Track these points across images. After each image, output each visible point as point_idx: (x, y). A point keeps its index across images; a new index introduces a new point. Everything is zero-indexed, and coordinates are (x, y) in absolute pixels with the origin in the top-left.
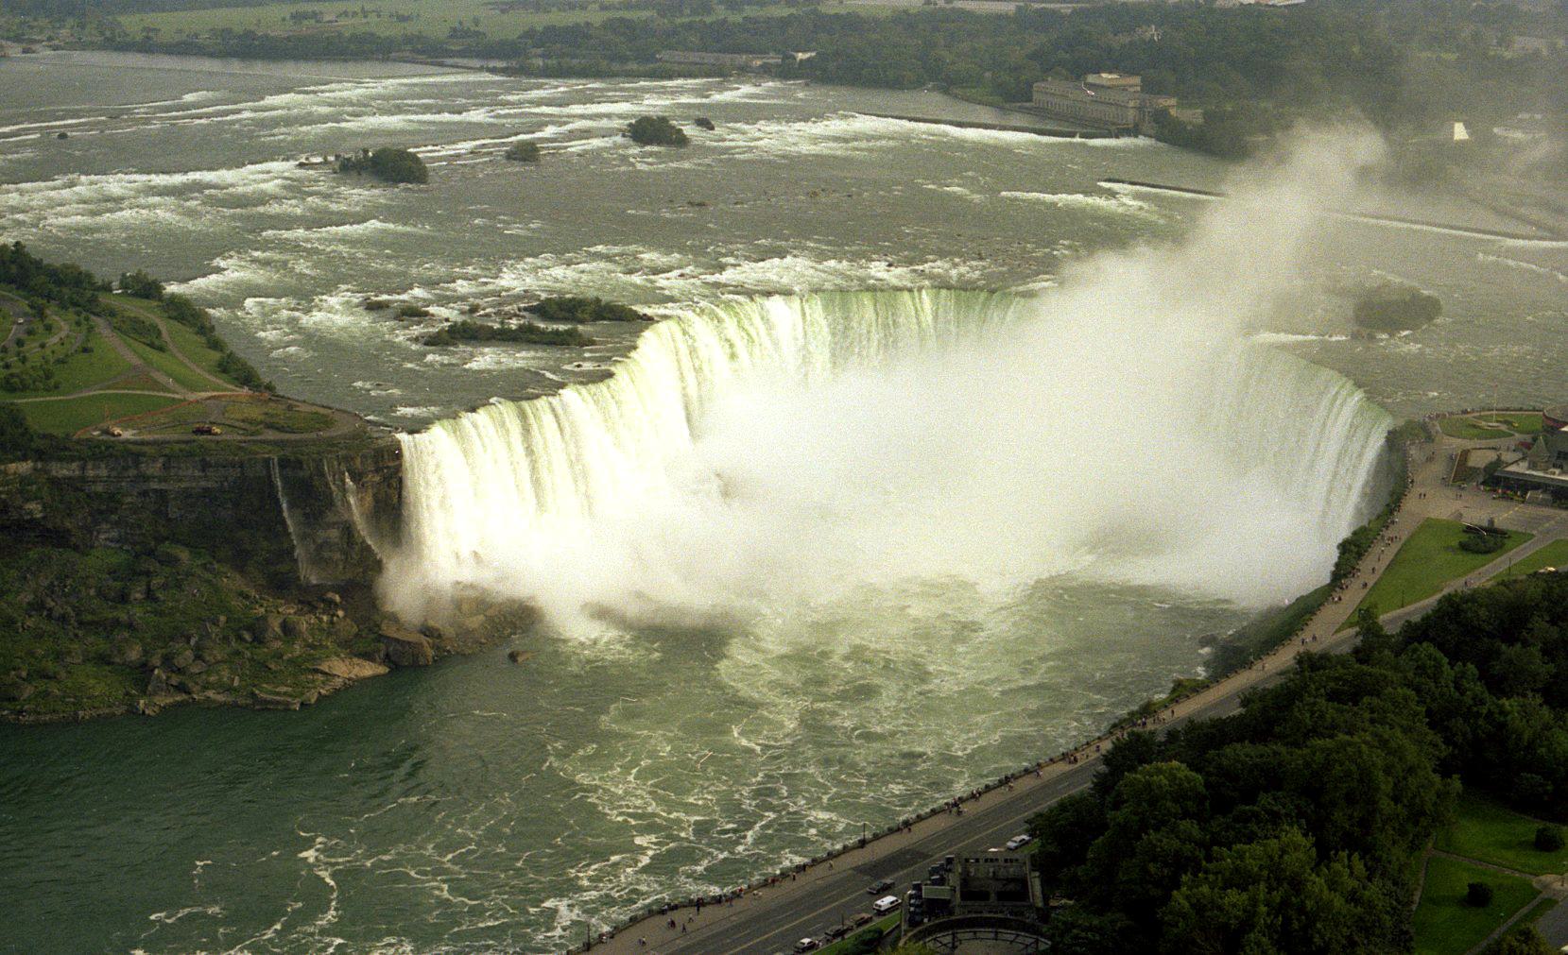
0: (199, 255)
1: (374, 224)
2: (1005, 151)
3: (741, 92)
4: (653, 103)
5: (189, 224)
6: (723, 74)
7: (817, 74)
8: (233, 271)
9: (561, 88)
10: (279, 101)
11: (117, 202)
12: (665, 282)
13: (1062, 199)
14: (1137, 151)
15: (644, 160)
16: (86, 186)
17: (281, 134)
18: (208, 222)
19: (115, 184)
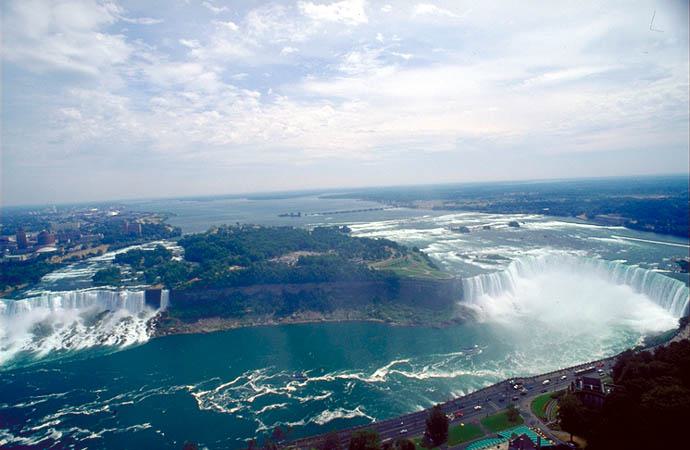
0: (426, 244)
1: (459, 240)
2: (588, 229)
3: (530, 217)
4: (512, 219)
5: (426, 239)
6: (527, 213)
7: (547, 213)
8: (432, 247)
9: (495, 215)
10: (441, 218)
11: (411, 234)
12: (515, 253)
13: (602, 239)
14: (619, 230)
15: (511, 229)
16: (407, 231)
17: (441, 224)
18: (426, 238)
19: (413, 231)
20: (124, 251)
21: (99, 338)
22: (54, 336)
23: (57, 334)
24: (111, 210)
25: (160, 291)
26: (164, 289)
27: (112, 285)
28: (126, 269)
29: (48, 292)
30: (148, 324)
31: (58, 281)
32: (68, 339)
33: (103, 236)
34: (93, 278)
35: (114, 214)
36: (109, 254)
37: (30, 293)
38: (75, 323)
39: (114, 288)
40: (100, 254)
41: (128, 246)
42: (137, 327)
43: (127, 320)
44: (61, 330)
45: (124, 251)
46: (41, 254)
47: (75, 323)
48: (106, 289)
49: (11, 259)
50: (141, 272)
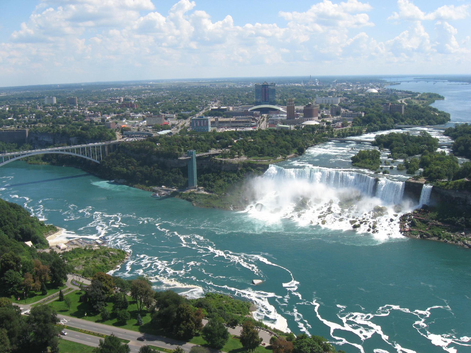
20: (385, 133)
21: (352, 222)
22: (312, 210)
23: (315, 208)
24: (372, 87)
25: (421, 185)
26: (426, 183)
27: (370, 169)
28: (385, 155)
29: (311, 166)
30: (403, 219)
31: (319, 156)
32: (324, 216)
33: (363, 115)
34: (352, 158)
35: (375, 91)
36: (368, 135)
37: (296, 163)
38: (331, 202)
39: (372, 173)
40: (360, 134)
41: (389, 129)
42: (392, 220)
43: (379, 211)
44: (319, 206)
45: (385, 133)
46: (308, 126)
47: (331, 202)
48: (364, 173)
49: (282, 128)
50: (401, 161)
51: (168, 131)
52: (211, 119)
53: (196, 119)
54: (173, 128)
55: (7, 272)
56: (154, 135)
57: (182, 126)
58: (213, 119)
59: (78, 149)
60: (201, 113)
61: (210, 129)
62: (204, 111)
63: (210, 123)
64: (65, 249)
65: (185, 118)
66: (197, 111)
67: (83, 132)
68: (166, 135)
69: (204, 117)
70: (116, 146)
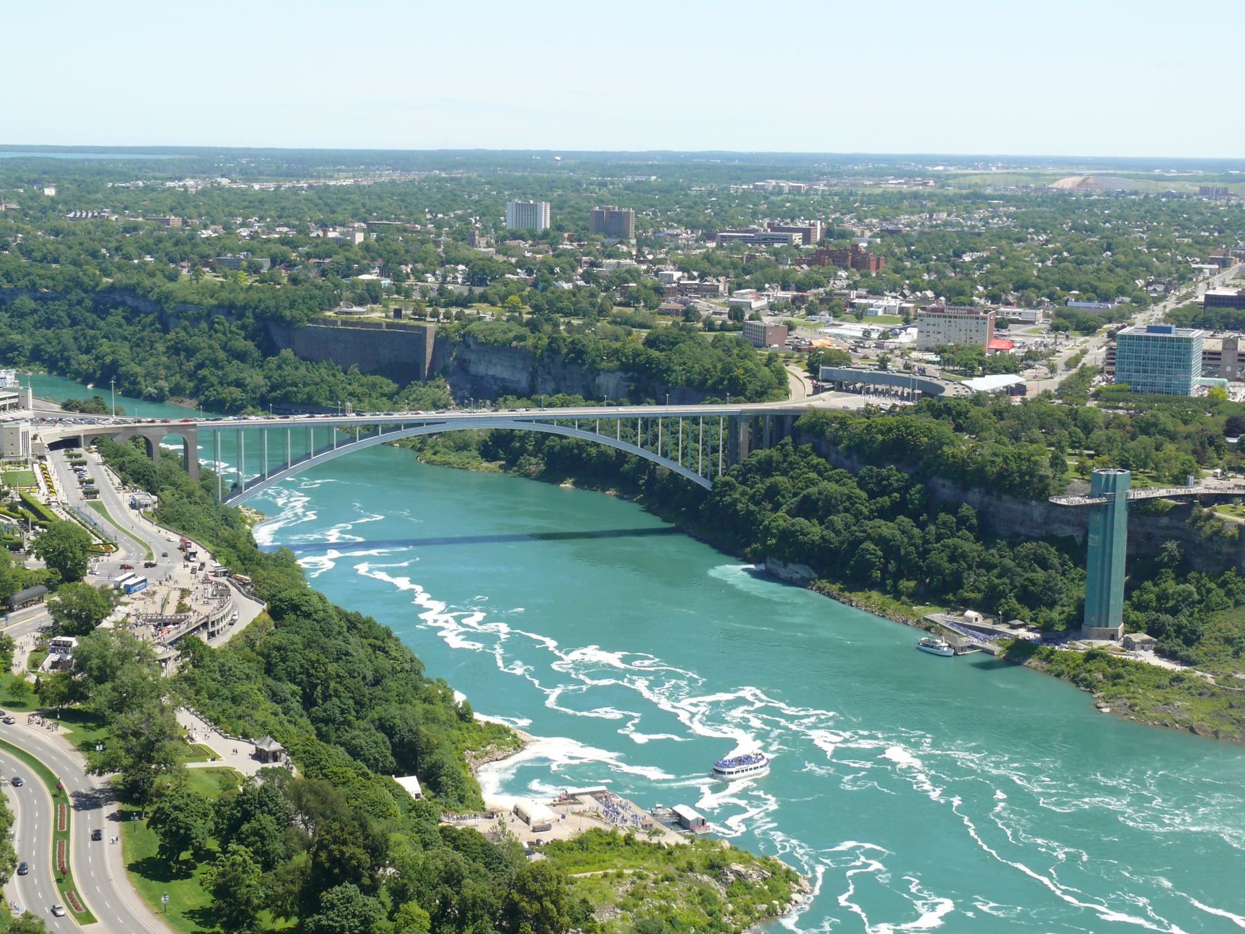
51: (1011, 380)
52: (1205, 341)
53: (1139, 338)
54: (1030, 367)
55: (337, 889)
56: (950, 391)
57: (1070, 364)
58: (1214, 343)
59: (631, 422)
60: (1156, 313)
61: (1198, 384)
62: (1171, 304)
63: (1197, 361)
64: (546, 828)
65: (1088, 329)
66: (1141, 303)
67: (655, 353)
68: (999, 395)
69: (1177, 333)
70: (785, 424)
